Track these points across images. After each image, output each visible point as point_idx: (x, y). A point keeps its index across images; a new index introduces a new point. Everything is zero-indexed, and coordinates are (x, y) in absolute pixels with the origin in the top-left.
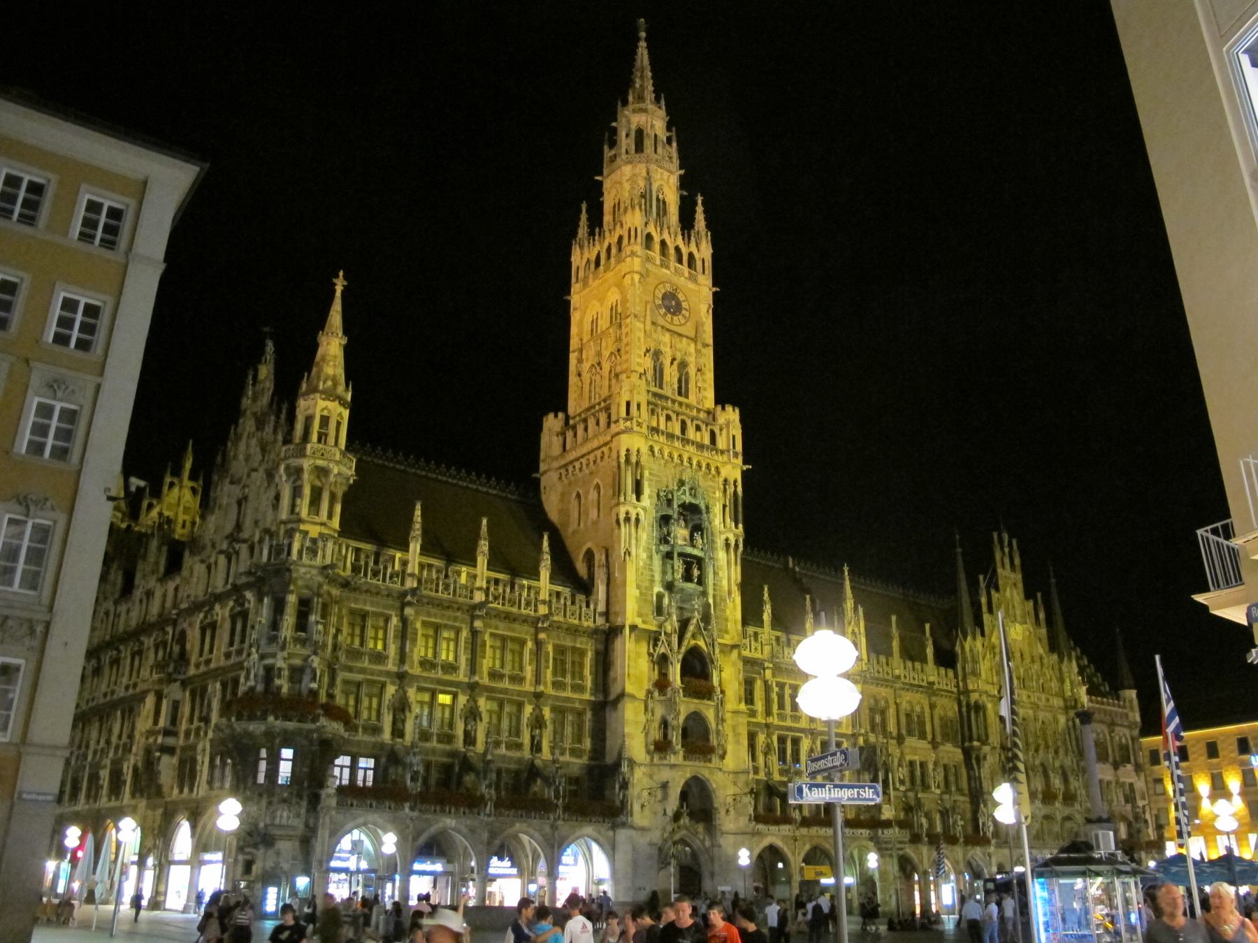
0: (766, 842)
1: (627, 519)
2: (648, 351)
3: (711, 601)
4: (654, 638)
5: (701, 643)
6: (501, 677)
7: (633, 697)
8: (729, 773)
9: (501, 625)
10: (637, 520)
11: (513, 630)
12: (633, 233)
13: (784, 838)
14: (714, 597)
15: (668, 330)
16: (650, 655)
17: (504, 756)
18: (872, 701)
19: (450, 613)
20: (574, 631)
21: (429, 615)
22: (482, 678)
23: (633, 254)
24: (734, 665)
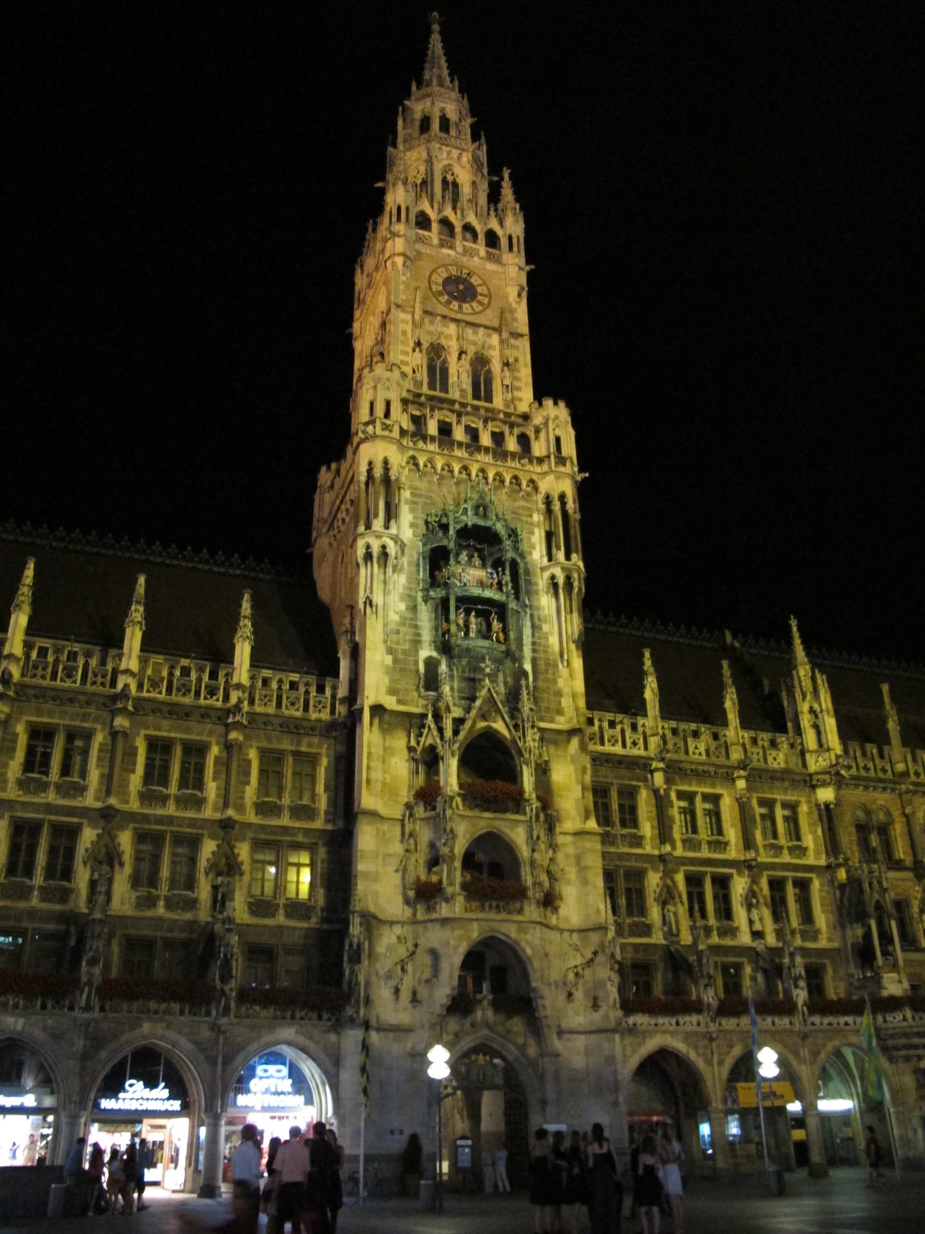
0: (652, 1044)
1: (368, 556)
2: (418, 344)
3: (528, 667)
4: (415, 723)
5: (499, 726)
6: (164, 799)
7: (374, 815)
8: (572, 931)
9: (165, 723)
10: (384, 554)
11: (187, 730)
12: (395, 212)
13: (687, 1037)
14: (534, 661)
15: (454, 320)
16: (410, 749)
17: (160, 919)
18: (860, 814)
19: (74, 709)
20: (294, 728)
21: (40, 713)
22: (127, 802)
23: (394, 235)
24: (573, 761)
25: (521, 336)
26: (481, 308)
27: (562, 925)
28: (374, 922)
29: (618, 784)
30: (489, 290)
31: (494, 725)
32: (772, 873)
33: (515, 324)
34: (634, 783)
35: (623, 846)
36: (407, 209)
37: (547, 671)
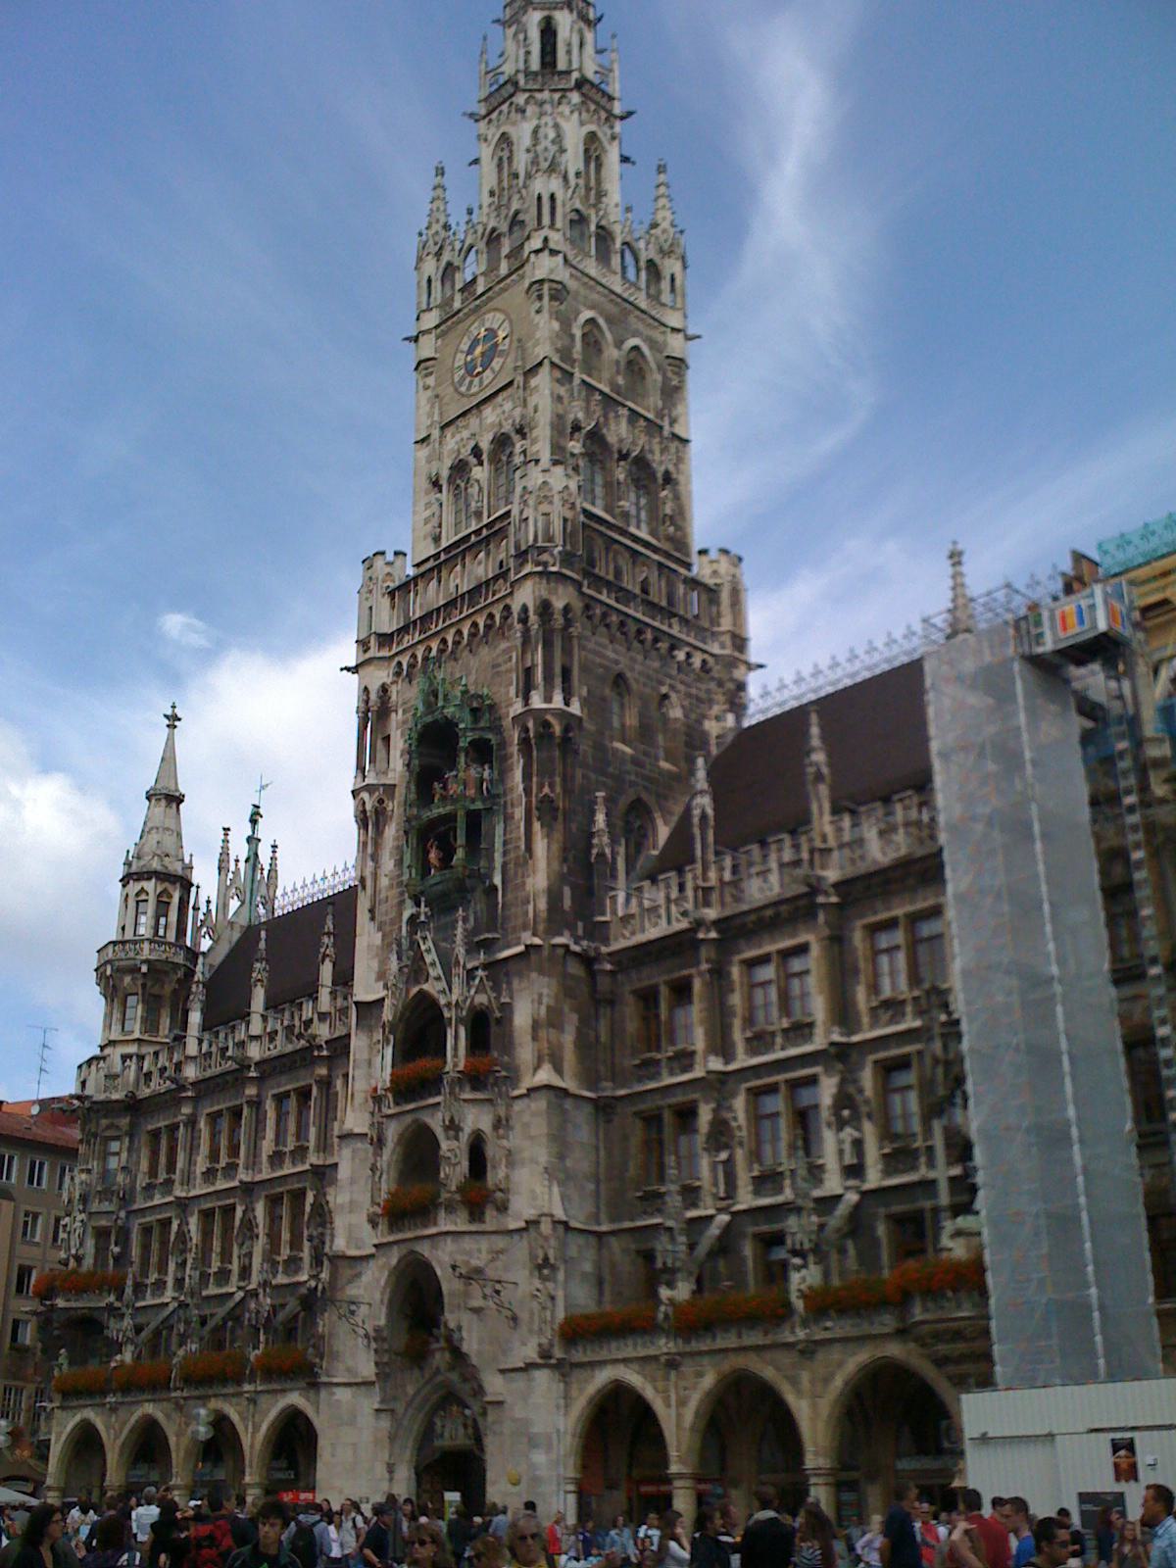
0: (603, 1377)
3: (497, 880)
9: (283, 1079)
14: (504, 866)
22: (260, 1171)
25: (540, 364)
26: (501, 360)
27: (513, 1225)
28: (346, 1263)
29: (666, 983)
30: (511, 322)
31: (425, 987)
32: (882, 1055)
33: (537, 350)
34: (685, 972)
35: (672, 1073)
36: (429, 281)
37: (516, 874)
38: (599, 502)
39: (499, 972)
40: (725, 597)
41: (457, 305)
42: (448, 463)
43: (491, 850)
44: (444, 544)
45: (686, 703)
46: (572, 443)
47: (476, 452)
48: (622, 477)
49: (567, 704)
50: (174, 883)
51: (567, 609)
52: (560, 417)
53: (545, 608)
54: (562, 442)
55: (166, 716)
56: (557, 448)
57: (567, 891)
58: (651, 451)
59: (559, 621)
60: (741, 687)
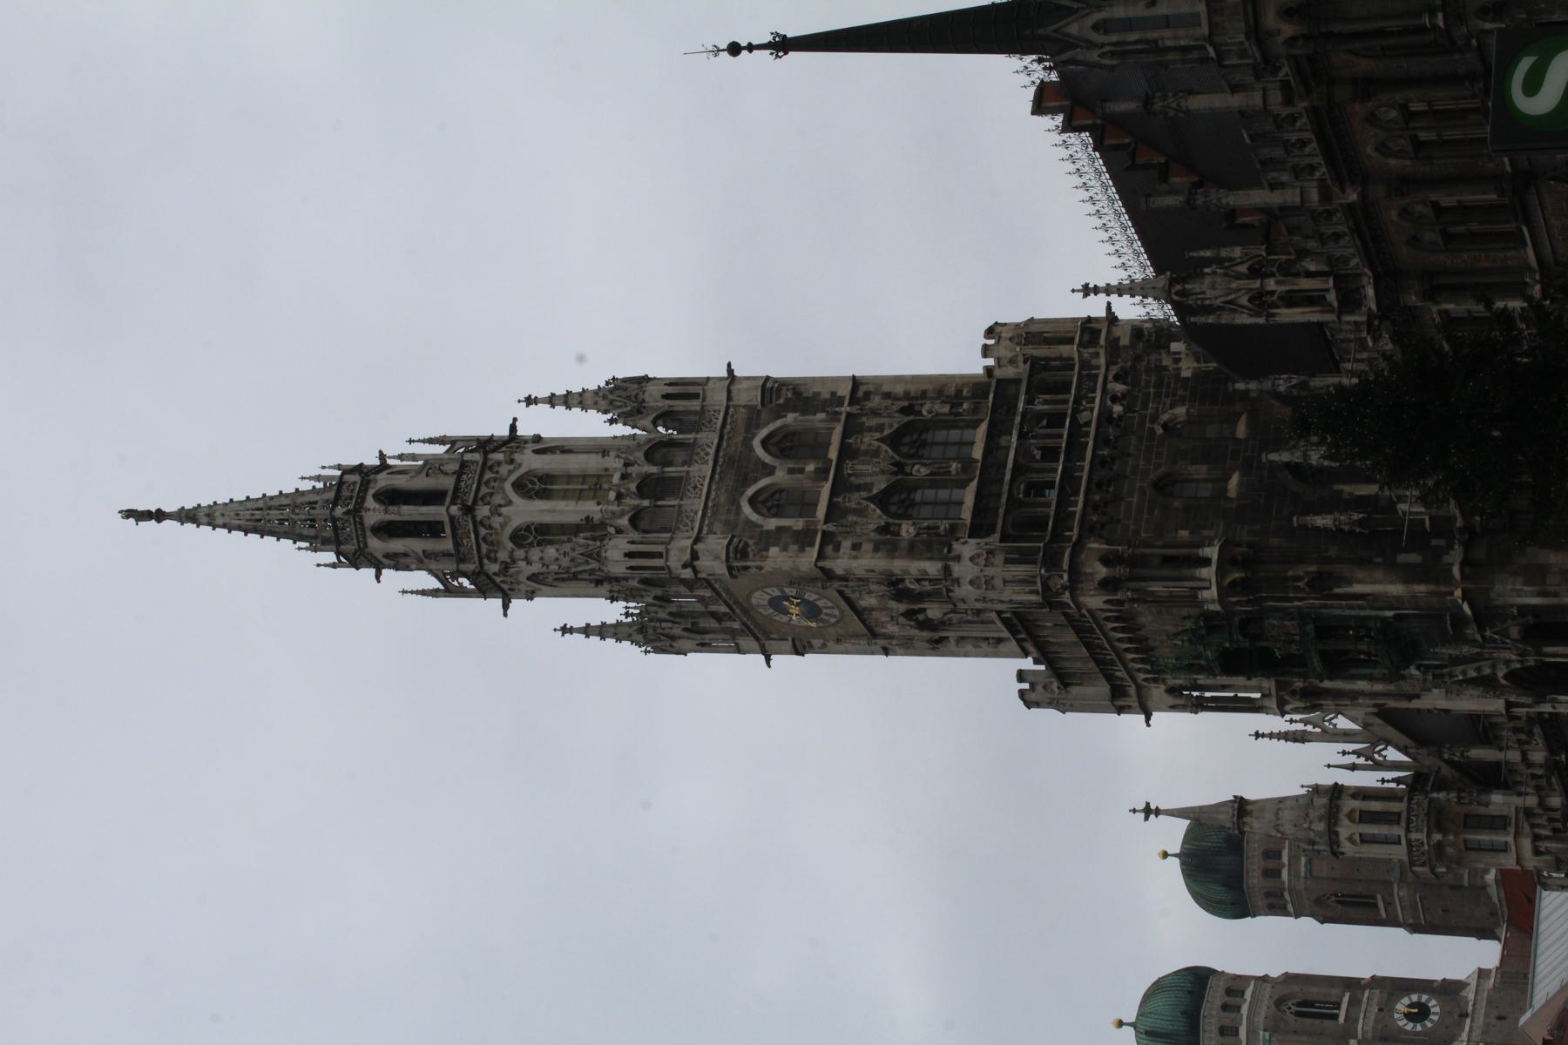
3: (1389, 614)
25: (821, 569)
38: (957, 494)
39: (1487, 615)
40: (1041, 351)
41: (736, 625)
42: (915, 632)
43: (1357, 618)
44: (1006, 634)
45: (1168, 401)
46: (903, 533)
47: (909, 614)
48: (924, 471)
49: (1206, 562)
50: (1338, 808)
51: (1105, 561)
52: (876, 549)
53: (1107, 585)
54: (904, 544)
55: (1146, 818)
56: (913, 550)
57: (1402, 558)
58: (880, 428)
59: (1120, 571)
60: (1137, 330)
